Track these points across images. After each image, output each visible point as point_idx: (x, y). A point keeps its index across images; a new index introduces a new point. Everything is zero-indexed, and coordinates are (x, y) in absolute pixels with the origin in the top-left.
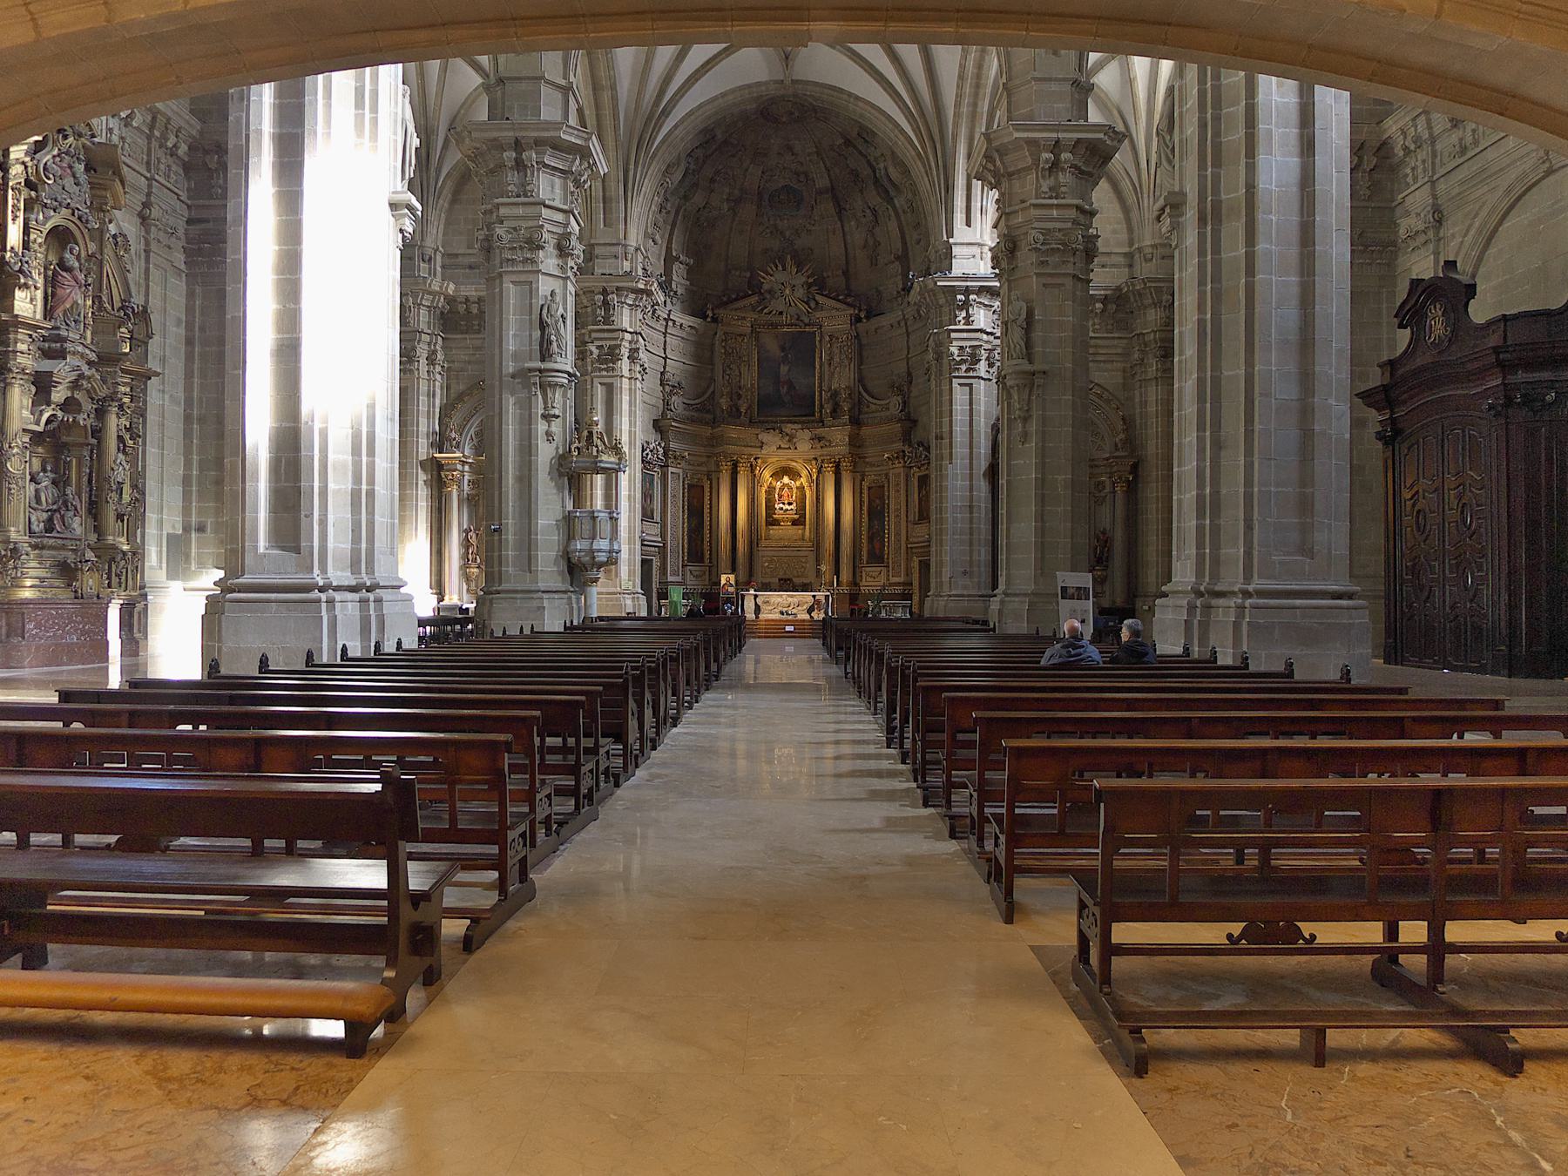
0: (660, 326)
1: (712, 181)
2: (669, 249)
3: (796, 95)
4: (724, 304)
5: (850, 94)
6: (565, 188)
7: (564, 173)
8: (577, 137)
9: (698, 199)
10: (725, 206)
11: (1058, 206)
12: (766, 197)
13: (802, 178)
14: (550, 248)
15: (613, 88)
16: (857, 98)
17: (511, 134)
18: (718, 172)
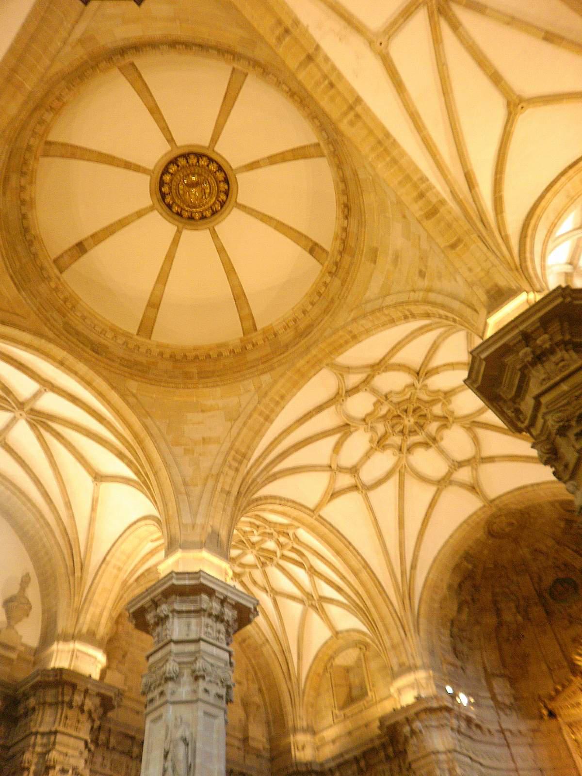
0: (497, 739)
1: (495, 602)
2: (485, 670)
3: (500, 509)
4: (552, 699)
5: (532, 485)
6: (199, 624)
7: (199, 612)
8: (190, 579)
9: (490, 620)
10: (519, 618)
11: (563, 380)
12: (547, 596)
13: (562, 566)
14: (186, 678)
15: (367, 566)
16: (538, 484)
17: (148, 598)
18: (494, 594)
